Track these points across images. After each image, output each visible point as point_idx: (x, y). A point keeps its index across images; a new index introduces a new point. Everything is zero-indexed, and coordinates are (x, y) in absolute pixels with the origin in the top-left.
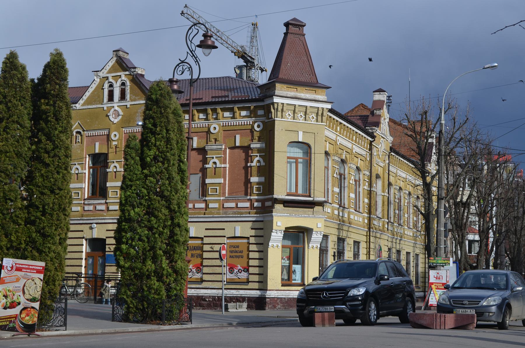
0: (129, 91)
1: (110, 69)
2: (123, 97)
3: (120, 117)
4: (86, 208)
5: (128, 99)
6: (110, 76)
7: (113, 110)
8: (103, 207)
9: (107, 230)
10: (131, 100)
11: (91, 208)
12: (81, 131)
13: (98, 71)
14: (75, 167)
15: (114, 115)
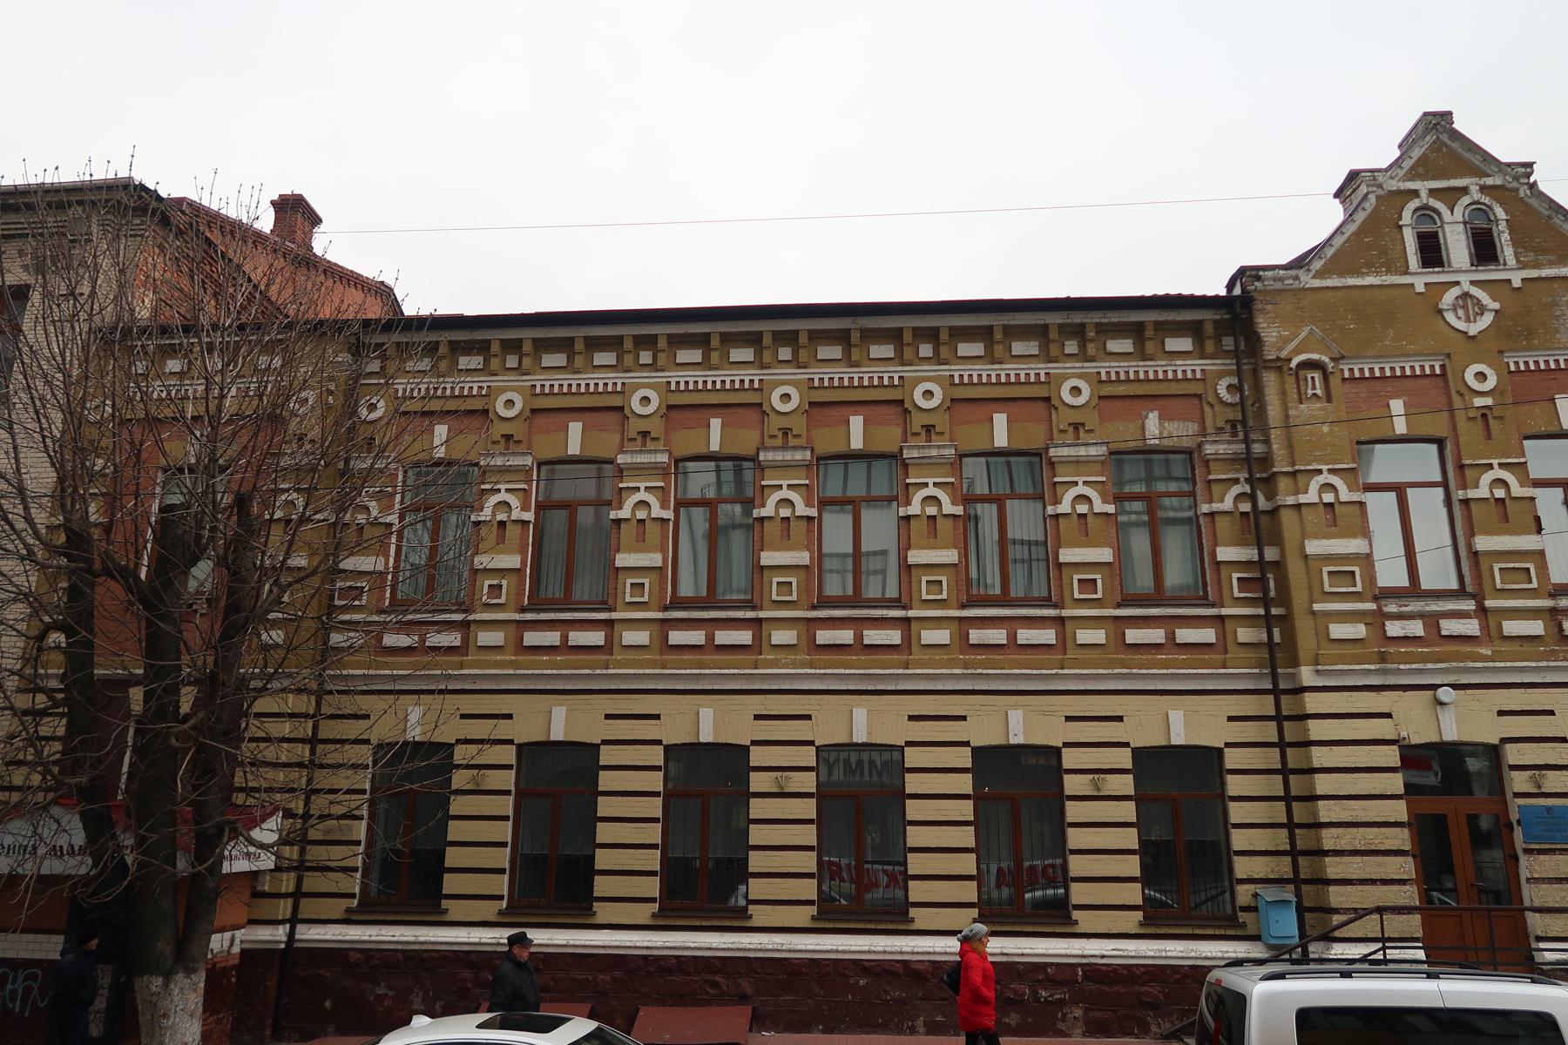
0: (1506, 237)
1: (1411, 169)
2: (1484, 250)
3: (1488, 319)
4: (1394, 629)
5: (1511, 261)
6: (1422, 186)
7: (1452, 294)
8: (1471, 627)
9: (1501, 713)
10: (1522, 266)
11: (1416, 628)
12: (1326, 359)
13: (1379, 170)
14: (1321, 479)
15: (1461, 312)
